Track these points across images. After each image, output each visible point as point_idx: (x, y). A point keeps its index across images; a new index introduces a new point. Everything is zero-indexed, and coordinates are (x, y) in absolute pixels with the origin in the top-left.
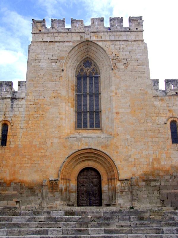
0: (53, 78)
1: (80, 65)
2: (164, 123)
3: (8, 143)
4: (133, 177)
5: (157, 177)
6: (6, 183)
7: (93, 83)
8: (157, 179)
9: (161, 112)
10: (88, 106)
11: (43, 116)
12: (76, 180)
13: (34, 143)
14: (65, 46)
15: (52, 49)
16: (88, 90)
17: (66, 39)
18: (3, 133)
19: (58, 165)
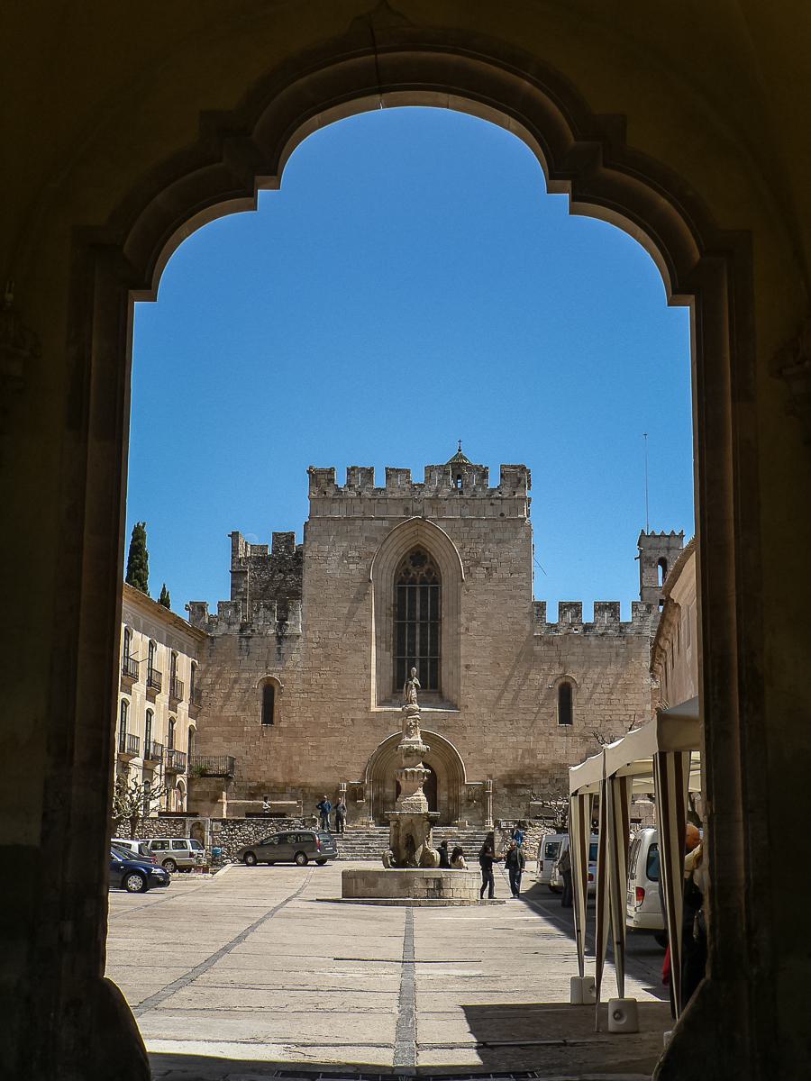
3: (275, 720)
10: (418, 647)
15: (349, 534)
16: (418, 613)
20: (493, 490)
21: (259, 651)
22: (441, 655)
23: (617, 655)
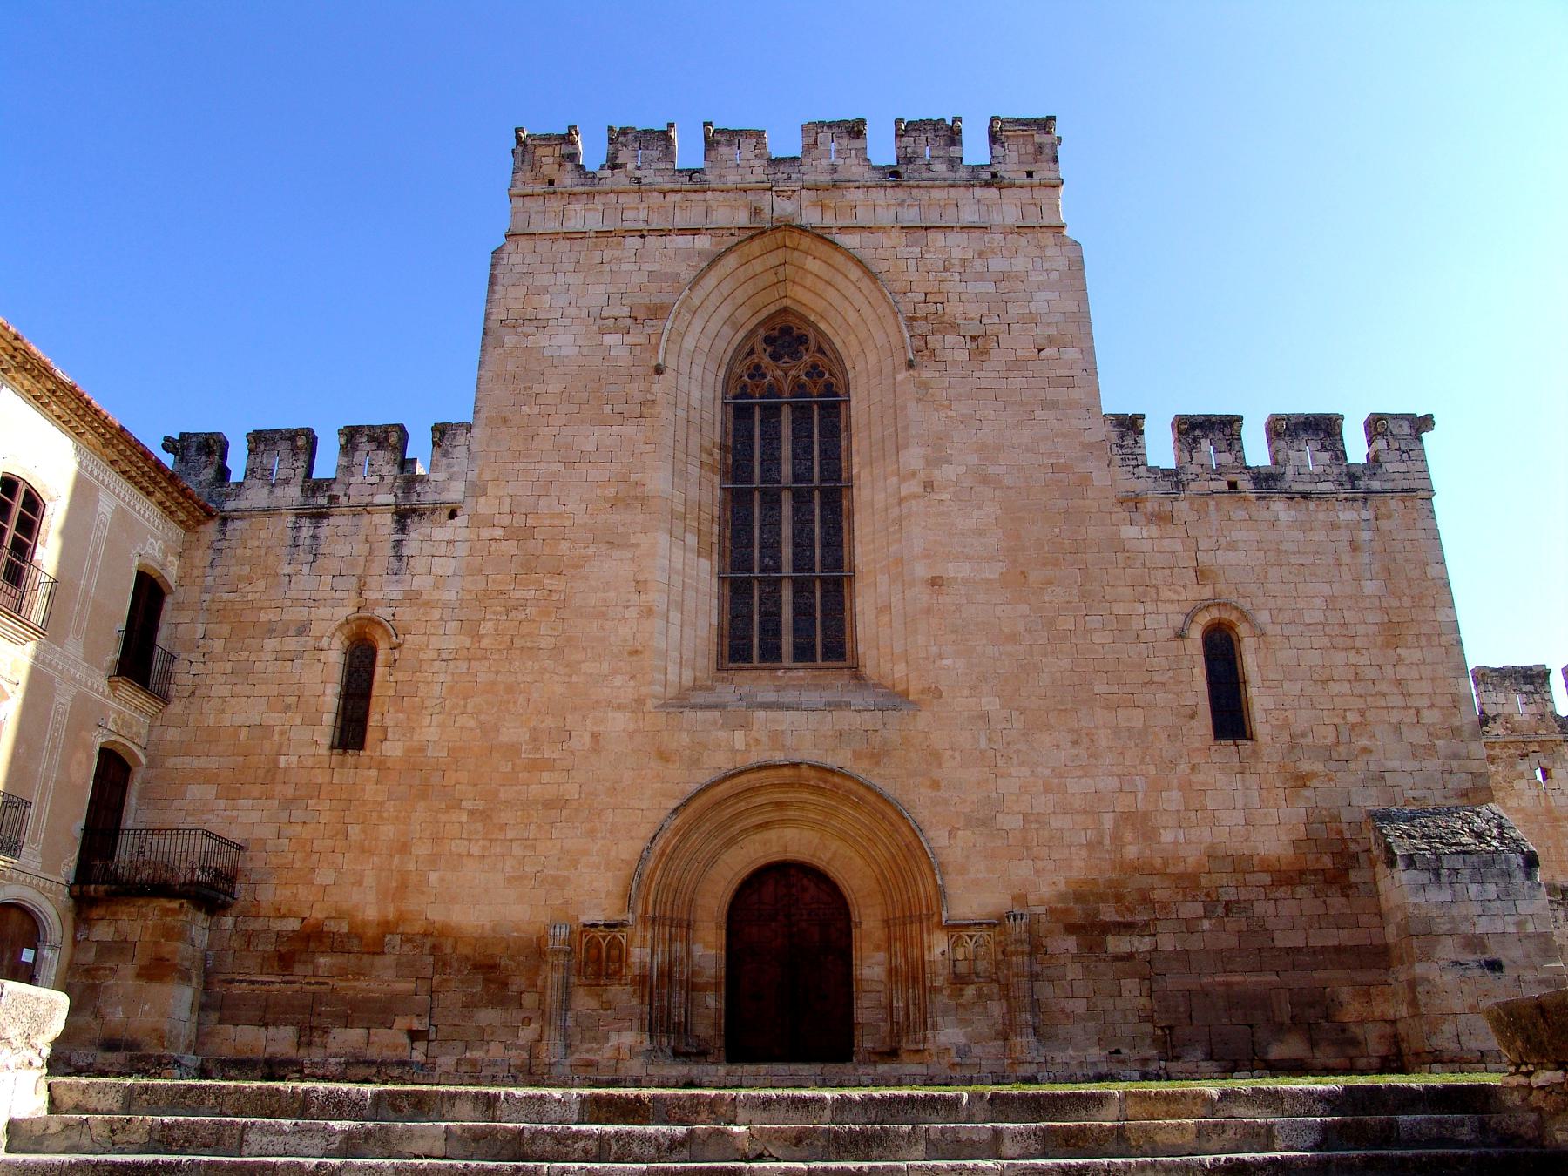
0: (608, 409)
1: (747, 349)
2: (1170, 633)
3: (372, 736)
4: (1017, 910)
5: (1139, 908)
6: (361, 939)
7: (810, 436)
8: (1141, 917)
9: (1159, 577)
10: (787, 552)
11: (555, 597)
12: (718, 927)
14: (671, 253)
15: (607, 268)
16: (787, 469)
17: (680, 221)
18: (348, 681)
19: (629, 849)
20: (974, 169)
21: (343, 550)
22: (852, 569)
23: (1354, 547)
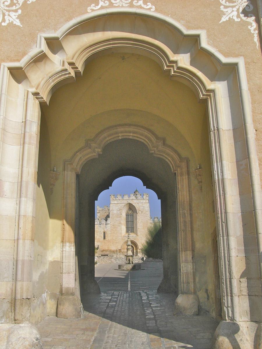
13: (114, 238)
